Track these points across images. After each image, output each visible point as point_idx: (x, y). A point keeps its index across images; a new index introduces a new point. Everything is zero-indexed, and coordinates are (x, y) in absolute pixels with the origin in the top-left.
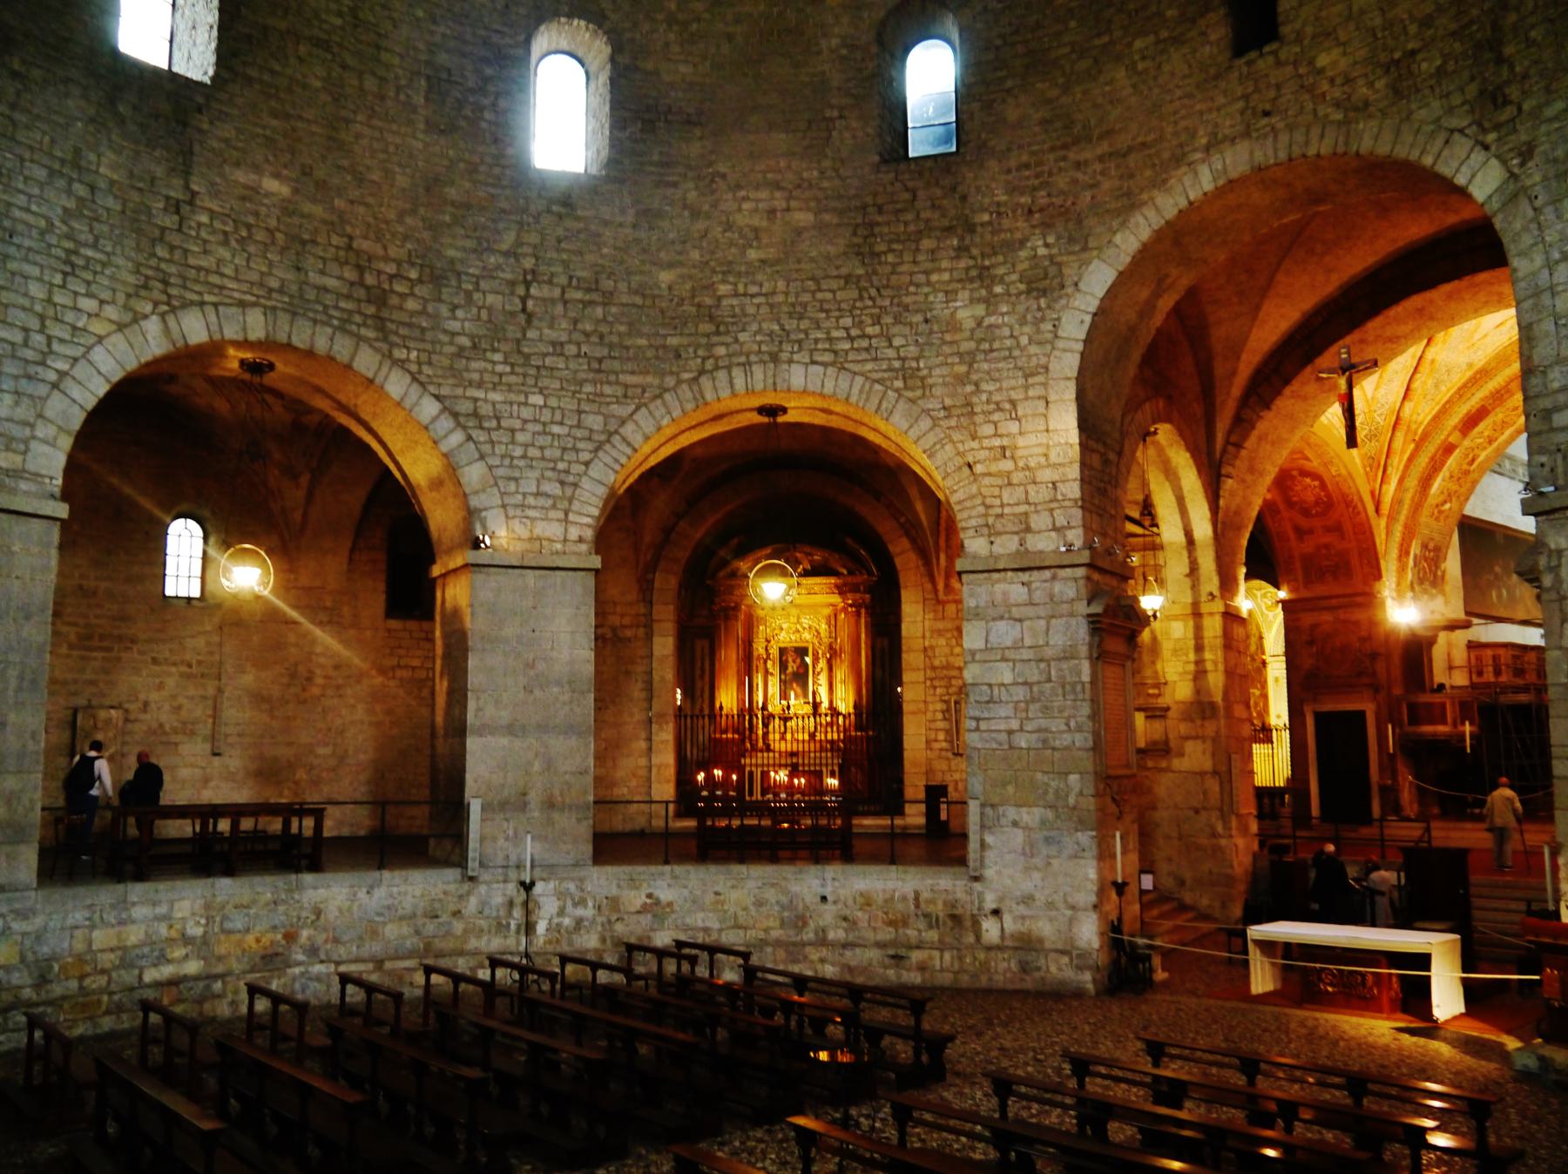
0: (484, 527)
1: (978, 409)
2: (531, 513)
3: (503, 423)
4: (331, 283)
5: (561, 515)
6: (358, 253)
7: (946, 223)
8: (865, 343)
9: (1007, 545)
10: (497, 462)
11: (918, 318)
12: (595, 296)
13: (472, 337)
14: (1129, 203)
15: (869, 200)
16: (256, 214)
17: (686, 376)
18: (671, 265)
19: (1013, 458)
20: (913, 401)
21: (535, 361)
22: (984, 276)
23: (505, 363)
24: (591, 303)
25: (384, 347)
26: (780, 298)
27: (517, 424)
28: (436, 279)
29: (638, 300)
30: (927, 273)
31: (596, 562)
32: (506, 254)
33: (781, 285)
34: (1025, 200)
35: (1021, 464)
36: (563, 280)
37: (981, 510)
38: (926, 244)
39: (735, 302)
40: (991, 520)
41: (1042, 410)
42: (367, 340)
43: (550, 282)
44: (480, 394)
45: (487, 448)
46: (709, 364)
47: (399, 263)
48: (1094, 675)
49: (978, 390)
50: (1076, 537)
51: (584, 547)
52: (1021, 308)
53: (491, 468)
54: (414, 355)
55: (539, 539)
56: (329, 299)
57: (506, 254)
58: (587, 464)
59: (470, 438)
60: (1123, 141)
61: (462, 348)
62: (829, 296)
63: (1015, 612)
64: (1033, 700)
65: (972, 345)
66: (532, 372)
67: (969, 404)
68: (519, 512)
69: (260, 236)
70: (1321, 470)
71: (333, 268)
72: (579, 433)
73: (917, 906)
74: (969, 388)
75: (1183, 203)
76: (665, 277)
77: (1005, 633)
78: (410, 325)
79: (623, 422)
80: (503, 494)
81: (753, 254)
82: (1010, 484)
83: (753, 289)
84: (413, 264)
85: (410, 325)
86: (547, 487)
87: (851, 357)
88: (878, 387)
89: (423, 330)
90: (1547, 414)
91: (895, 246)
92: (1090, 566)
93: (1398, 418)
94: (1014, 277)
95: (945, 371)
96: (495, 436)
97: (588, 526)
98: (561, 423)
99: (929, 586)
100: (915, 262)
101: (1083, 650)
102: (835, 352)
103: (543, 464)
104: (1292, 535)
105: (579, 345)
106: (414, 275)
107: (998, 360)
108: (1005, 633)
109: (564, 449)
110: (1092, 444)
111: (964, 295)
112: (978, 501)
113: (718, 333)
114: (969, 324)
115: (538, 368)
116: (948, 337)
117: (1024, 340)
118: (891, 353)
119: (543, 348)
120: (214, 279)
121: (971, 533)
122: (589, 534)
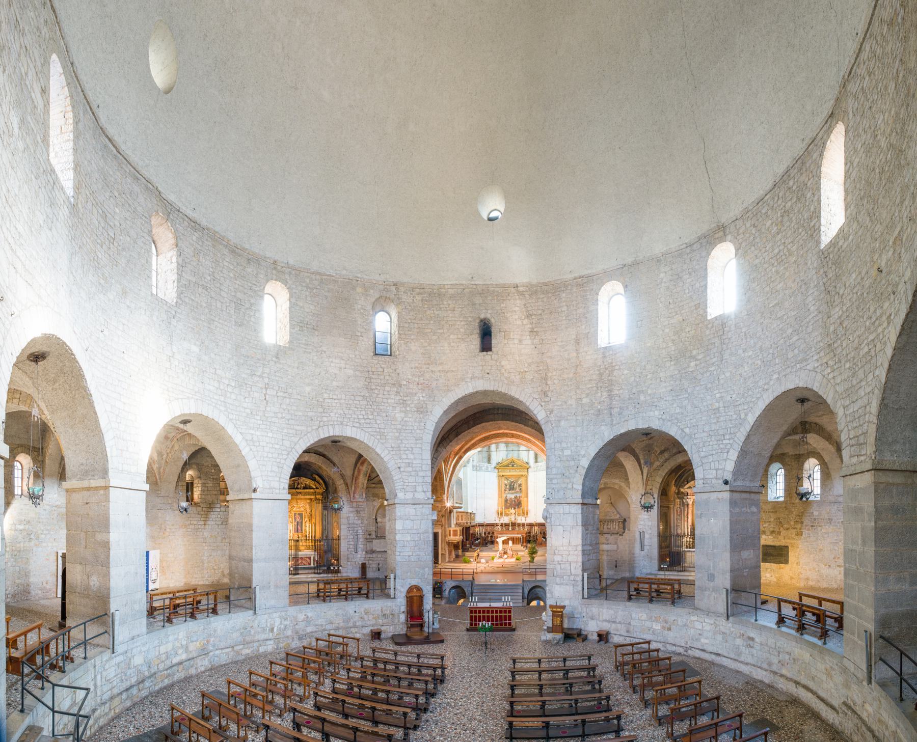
8: (368, 421)
9: (409, 496)
11: (384, 415)
12: (286, 395)
15: (370, 369)
17: (314, 428)
19: (412, 467)
29: (299, 397)
33: (343, 396)
34: (417, 379)
38: (387, 388)
39: (329, 401)
49: (402, 443)
62: (358, 402)
63: (412, 518)
64: (416, 546)
73: (382, 612)
74: (399, 442)
76: (308, 389)
77: (409, 524)
79: (295, 444)
83: (335, 397)
87: (365, 425)
94: (413, 405)
108: (409, 524)
111: (398, 409)
114: (399, 419)
118: (376, 426)
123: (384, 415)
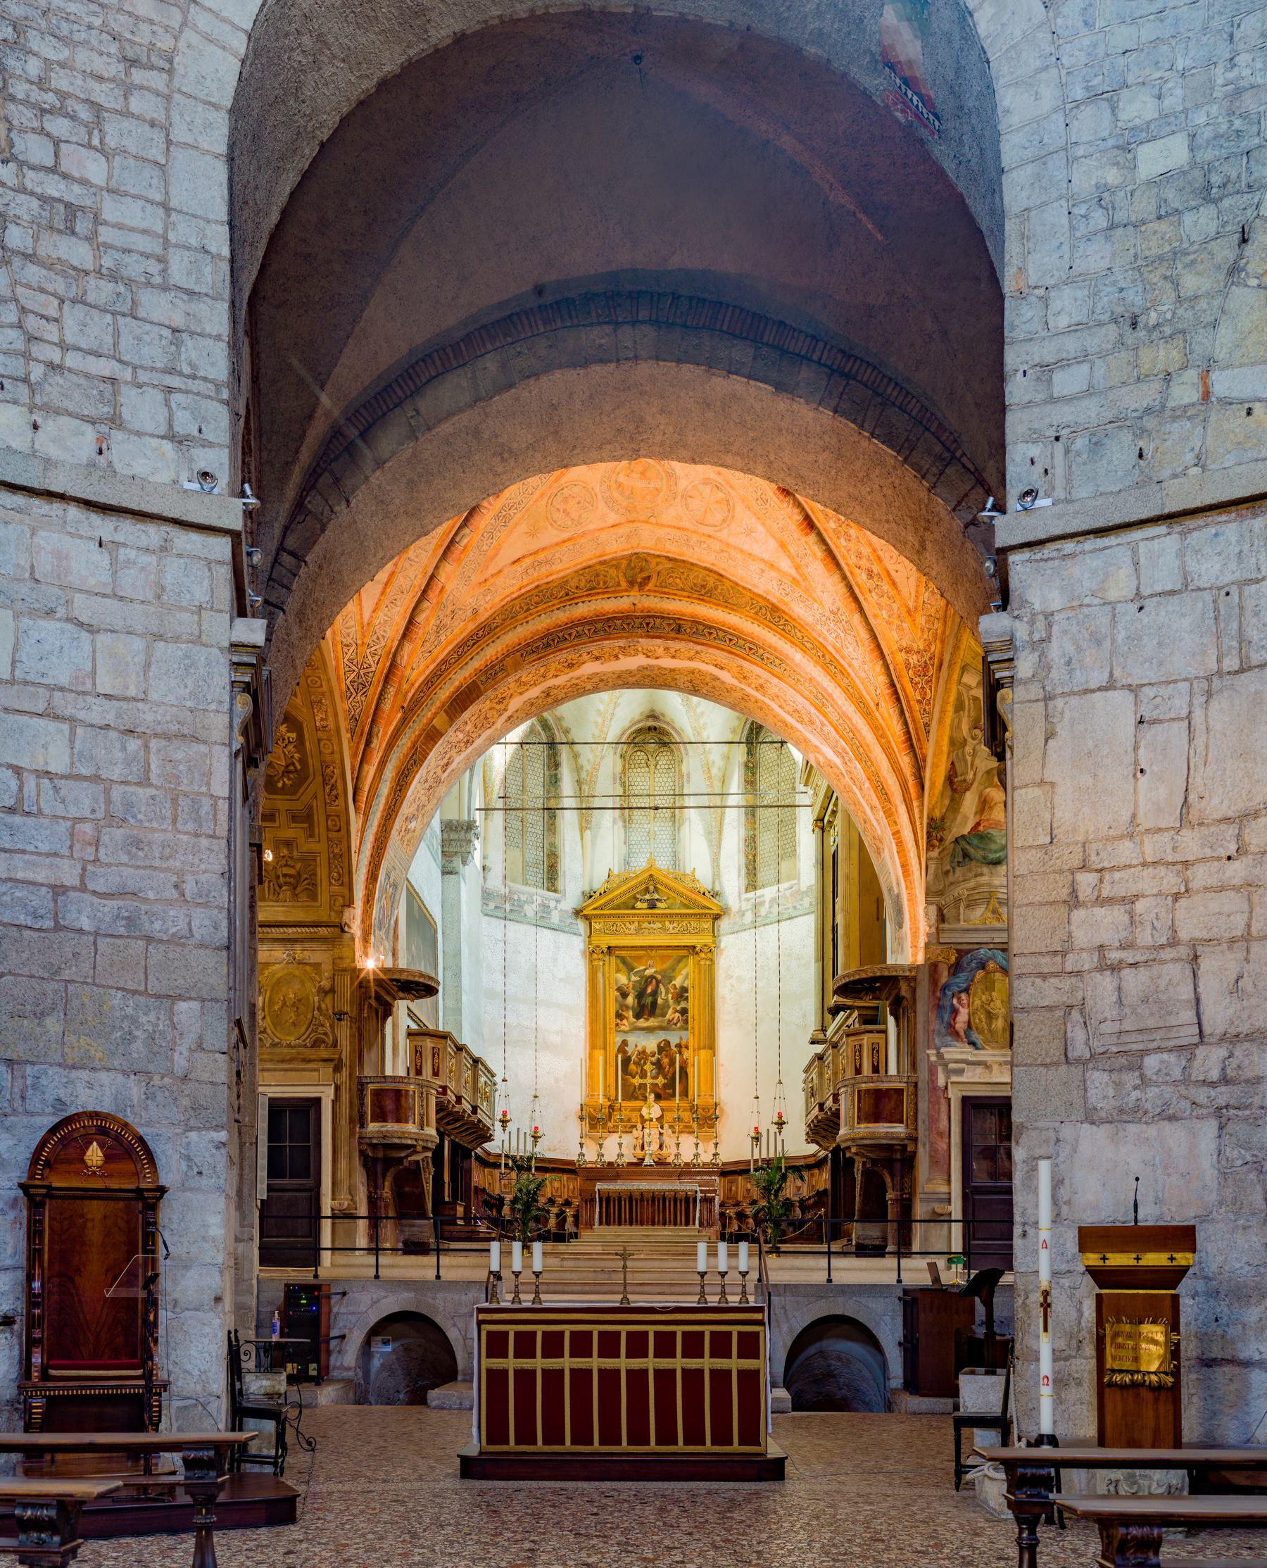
1: (19, 89)
19: (91, 238)
35: (107, 262)
40: (37, 372)
63: (83, 607)
82: (80, 300)
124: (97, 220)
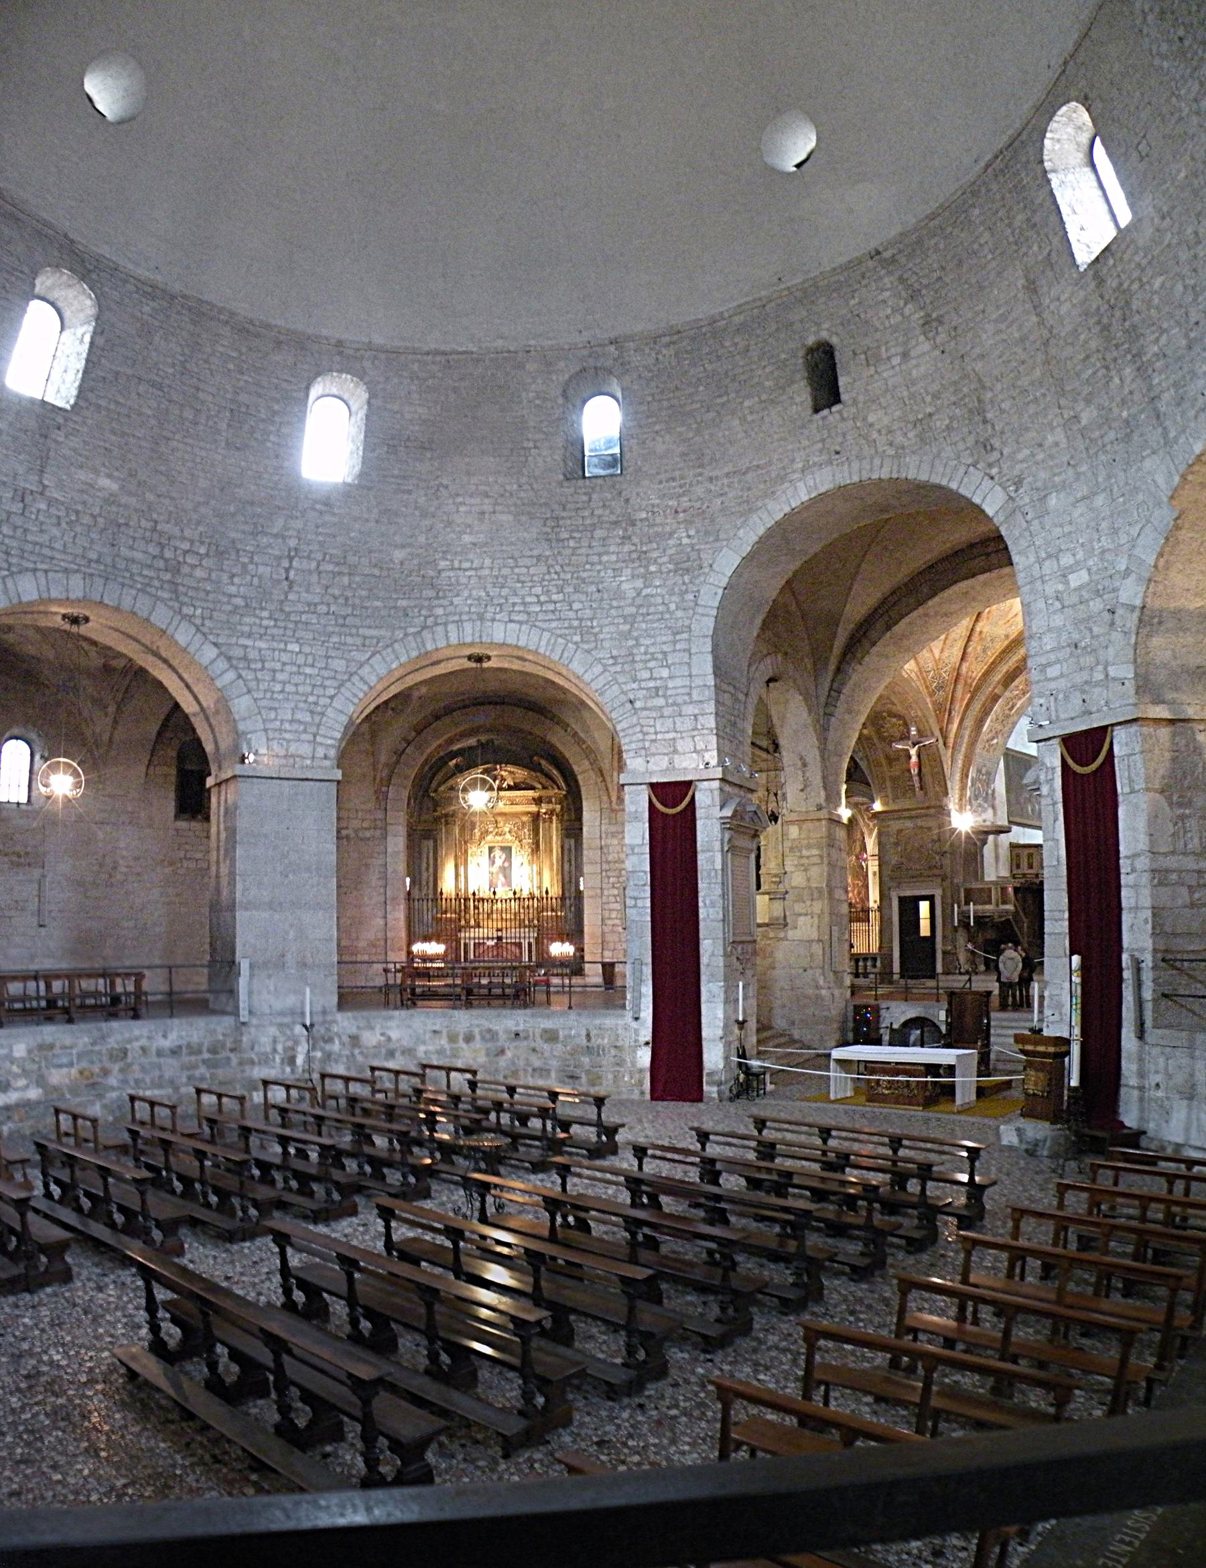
0: (250, 749)
1: (637, 658)
2: (287, 736)
3: (267, 665)
4: (138, 556)
5: (311, 737)
6: (161, 534)
7: (613, 518)
8: (551, 607)
10: (261, 695)
11: (593, 588)
13: (244, 598)
14: (748, 509)
16: (84, 503)
17: (411, 630)
18: (403, 546)
19: (664, 696)
20: (588, 651)
21: (293, 617)
22: (642, 557)
23: (270, 618)
24: (340, 573)
25: (176, 605)
26: (487, 572)
27: (278, 666)
28: (220, 554)
29: (376, 572)
30: (600, 555)
31: (338, 775)
32: (275, 536)
33: (488, 562)
36: (319, 556)
37: (640, 736)
38: (599, 533)
39: (451, 574)
40: (647, 744)
41: (686, 660)
42: (163, 600)
43: (308, 557)
44: (249, 642)
45: (253, 684)
46: (430, 621)
47: (192, 542)
48: (724, 863)
49: (638, 645)
50: (712, 757)
51: (327, 763)
52: (670, 583)
53: (255, 700)
54: (199, 611)
55: (292, 756)
56: (135, 569)
57: (275, 536)
58: (332, 698)
59: (240, 676)
60: (744, 464)
61: (236, 607)
62: (524, 570)
65: (633, 610)
66: (291, 626)
67: (631, 654)
68: (277, 735)
69: (86, 520)
70: (903, 712)
71: (140, 544)
72: (325, 673)
74: (631, 643)
75: (787, 509)
76: (399, 555)
78: (197, 589)
79: (361, 666)
80: (264, 721)
81: (467, 538)
83: (466, 565)
84: (202, 543)
85: (197, 589)
86: (299, 716)
87: (540, 617)
88: (560, 640)
89: (208, 593)
90: (1043, 668)
91: (576, 535)
92: (722, 780)
93: (958, 675)
94: (665, 559)
95: (612, 629)
96: (259, 675)
97: (332, 746)
98: (313, 666)
99: (605, 798)
100: (590, 547)
101: (717, 845)
102: (528, 614)
103: (298, 697)
104: (884, 762)
105: (328, 605)
106: (203, 550)
107: (652, 621)
109: (314, 686)
110: (725, 687)
112: (638, 729)
113: (437, 598)
115: (296, 623)
116: (615, 603)
117: (673, 607)
118: (571, 614)
119: (300, 607)
120: (46, 551)
121: (632, 754)
122: (332, 753)
123: (593, 588)
124: (667, 688)
